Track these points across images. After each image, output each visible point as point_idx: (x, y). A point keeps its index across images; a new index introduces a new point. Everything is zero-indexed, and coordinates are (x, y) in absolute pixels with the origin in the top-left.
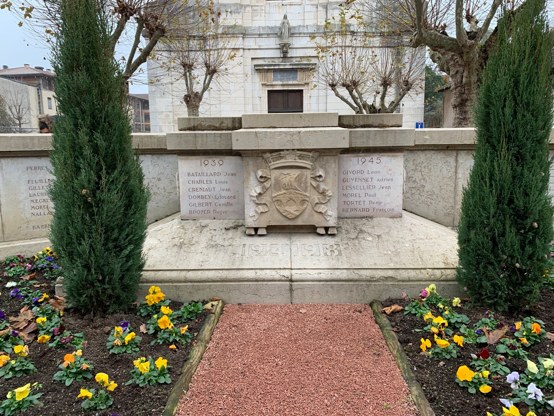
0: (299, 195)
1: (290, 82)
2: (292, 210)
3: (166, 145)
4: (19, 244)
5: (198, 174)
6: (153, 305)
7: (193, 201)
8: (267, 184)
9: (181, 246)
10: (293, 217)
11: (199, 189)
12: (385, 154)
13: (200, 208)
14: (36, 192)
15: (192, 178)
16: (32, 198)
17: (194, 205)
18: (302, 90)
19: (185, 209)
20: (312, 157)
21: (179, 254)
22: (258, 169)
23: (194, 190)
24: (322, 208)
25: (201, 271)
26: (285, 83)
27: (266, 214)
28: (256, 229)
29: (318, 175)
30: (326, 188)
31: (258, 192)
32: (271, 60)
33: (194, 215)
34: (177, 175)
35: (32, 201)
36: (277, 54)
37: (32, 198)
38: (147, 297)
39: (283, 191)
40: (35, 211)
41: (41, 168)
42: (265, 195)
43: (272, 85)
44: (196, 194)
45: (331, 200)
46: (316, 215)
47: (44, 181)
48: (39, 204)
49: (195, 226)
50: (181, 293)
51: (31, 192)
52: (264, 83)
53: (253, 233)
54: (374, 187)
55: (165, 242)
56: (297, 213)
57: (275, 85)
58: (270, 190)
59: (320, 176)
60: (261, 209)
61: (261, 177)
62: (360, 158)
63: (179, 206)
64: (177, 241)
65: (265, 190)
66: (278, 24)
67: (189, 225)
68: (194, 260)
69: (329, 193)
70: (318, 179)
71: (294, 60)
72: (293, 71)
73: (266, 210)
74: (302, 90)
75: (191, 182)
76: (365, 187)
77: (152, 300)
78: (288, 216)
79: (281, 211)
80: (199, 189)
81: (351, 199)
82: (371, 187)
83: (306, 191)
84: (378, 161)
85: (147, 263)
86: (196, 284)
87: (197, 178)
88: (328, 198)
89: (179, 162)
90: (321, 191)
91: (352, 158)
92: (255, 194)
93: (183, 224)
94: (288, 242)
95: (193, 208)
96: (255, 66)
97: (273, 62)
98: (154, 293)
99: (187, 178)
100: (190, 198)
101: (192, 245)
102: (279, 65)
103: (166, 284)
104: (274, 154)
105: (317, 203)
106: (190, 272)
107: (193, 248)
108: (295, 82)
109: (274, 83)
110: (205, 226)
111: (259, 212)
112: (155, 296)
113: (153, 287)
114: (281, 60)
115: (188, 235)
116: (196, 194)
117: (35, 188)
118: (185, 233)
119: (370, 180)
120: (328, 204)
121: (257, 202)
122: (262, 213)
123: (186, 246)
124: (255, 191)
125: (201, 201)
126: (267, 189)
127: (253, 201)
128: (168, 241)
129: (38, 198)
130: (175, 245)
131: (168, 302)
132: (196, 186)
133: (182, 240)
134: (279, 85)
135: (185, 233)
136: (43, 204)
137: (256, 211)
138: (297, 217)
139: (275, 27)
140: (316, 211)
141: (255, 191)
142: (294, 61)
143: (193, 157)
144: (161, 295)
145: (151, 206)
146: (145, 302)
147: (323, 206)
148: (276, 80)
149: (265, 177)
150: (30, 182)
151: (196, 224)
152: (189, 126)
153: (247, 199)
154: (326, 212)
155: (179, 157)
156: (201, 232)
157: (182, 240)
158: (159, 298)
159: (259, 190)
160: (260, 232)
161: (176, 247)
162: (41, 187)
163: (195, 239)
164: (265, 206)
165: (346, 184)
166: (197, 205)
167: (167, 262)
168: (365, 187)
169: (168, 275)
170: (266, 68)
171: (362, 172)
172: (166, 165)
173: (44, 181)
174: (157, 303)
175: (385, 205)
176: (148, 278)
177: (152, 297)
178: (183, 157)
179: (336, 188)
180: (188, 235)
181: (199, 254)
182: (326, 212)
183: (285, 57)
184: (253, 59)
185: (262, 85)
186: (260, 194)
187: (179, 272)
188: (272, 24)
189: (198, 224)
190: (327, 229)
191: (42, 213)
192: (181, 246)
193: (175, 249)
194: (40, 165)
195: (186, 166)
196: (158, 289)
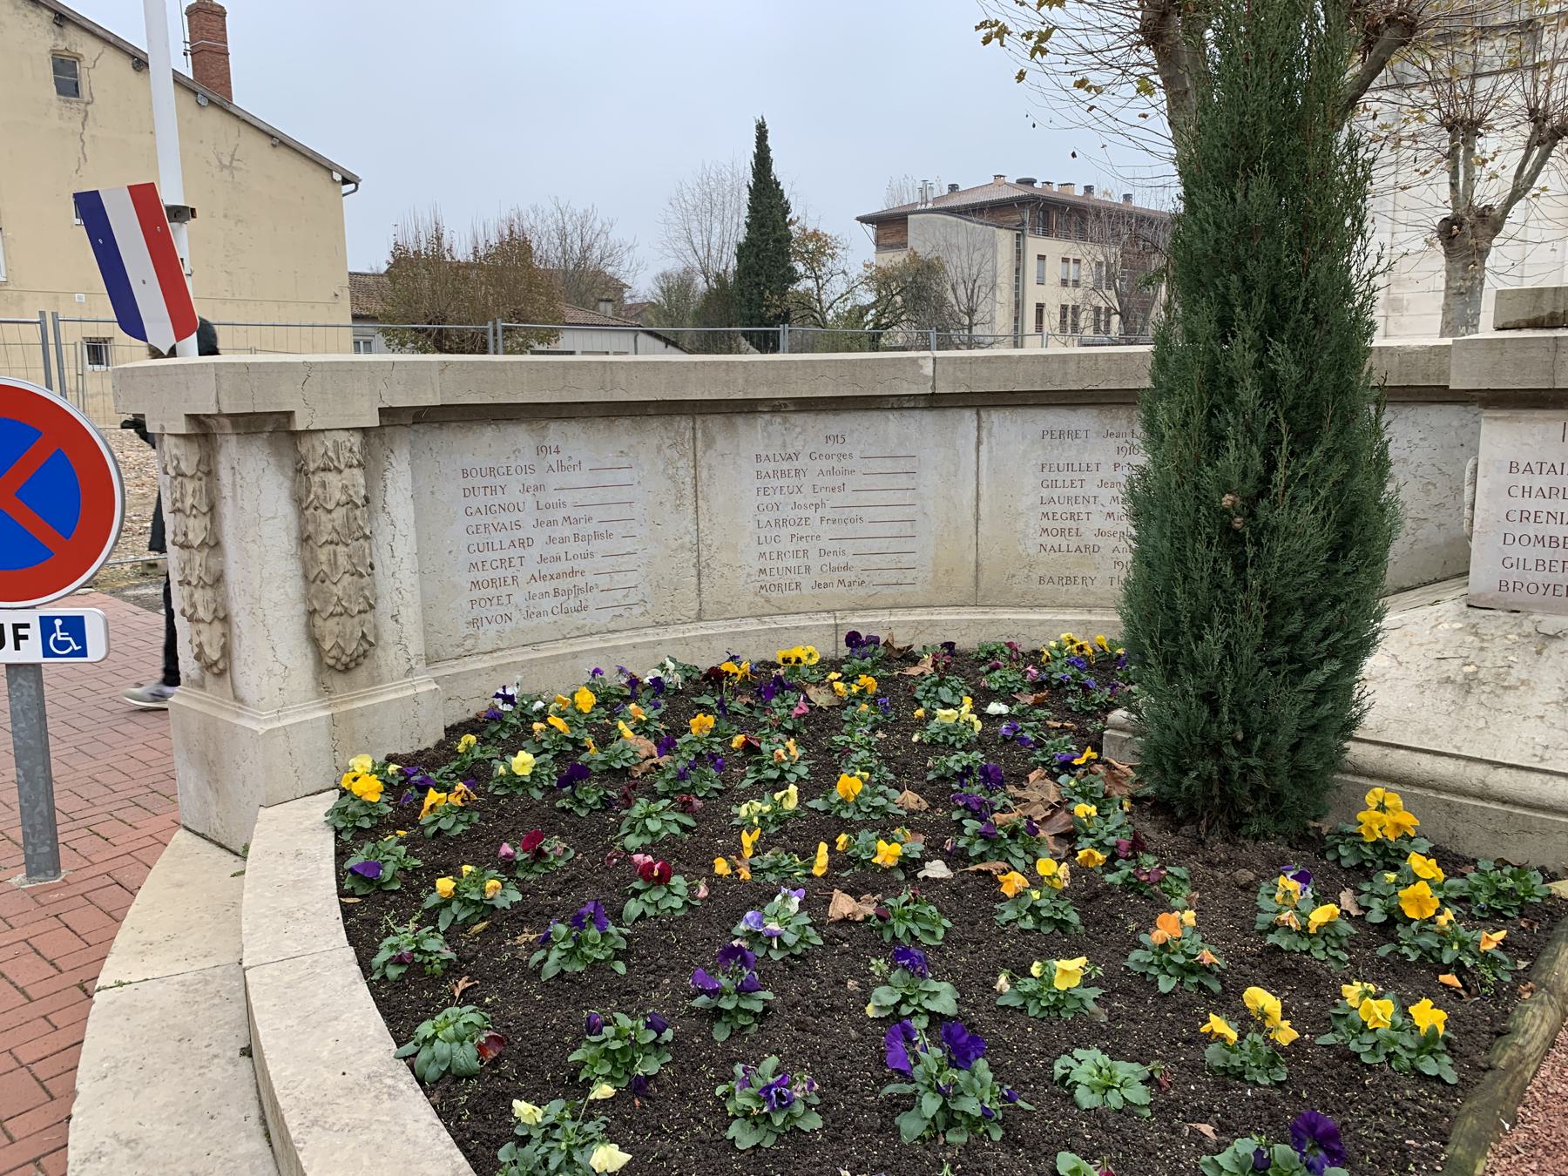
3: (1445, 373)
4: (1006, 616)
5: (1546, 468)
6: (1377, 844)
7: (1516, 552)
9: (1467, 685)
11: (1543, 517)
13: (1541, 577)
15: (1524, 480)
16: (1045, 508)
17: (1521, 564)
19: (1484, 572)
21: (1462, 708)
23: (1524, 516)
25: (1541, 776)
33: (1520, 597)
34: (1470, 464)
35: (1045, 515)
37: (1045, 508)
38: (1361, 816)
40: (1049, 541)
41: (1075, 435)
44: (1531, 529)
47: (1076, 467)
48: (1059, 525)
49: (1516, 630)
50: (1462, 829)
51: (1045, 493)
55: (1413, 667)
63: (1468, 563)
64: (1452, 668)
67: (1496, 625)
68: (1514, 736)
75: (1517, 492)
77: (1376, 827)
80: (1543, 517)
85: (1370, 720)
86: (1518, 811)
87: (1542, 481)
89: (1485, 428)
93: (1473, 621)
95: (1514, 575)
98: (1382, 808)
99: (1505, 478)
100: (1509, 540)
101: (1505, 688)
103: (1417, 791)
106: (1502, 771)
107: (1510, 699)
110: (1555, 637)
112: (1387, 819)
113: (1378, 790)
115: (1494, 657)
116: (1531, 529)
117: (1054, 484)
118: (1482, 649)
123: (1487, 689)
125: (1546, 554)
128: (1424, 665)
129: (1058, 509)
130: (1448, 680)
131: (1425, 845)
132: (1532, 504)
133: (1472, 669)
135: (1482, 649)
136: (1069, 524)
143: (1538, 414)
144: (1409, 820)
145: (1397, 551)
146: (1355, 829)
150: (1046, 469)
151: (1521, 625)
152: (1532, 316)
155: (1488, 413)
156: (1539, 653)
157: (1472, 669)
158: (1398, 826)
161: (1450, 687)
163: (1518, 673)
166: (1531, 564)
167: (1422, 727)
169: (1426, 765)
172: (1416, 436)
173: (1076, 467)
174: (1392, 838)
176: (1359, 762)
177: (1378, 820)
178: (1499, 414)
180: (1494, 657)
181: (1532, 722)
187: (1463, 763)
189: (1528, 627)
191: (1064, 548)
192: (1467, 685)
193: (1449, 693)
195: (1502, 441)
196: (1394, 800)
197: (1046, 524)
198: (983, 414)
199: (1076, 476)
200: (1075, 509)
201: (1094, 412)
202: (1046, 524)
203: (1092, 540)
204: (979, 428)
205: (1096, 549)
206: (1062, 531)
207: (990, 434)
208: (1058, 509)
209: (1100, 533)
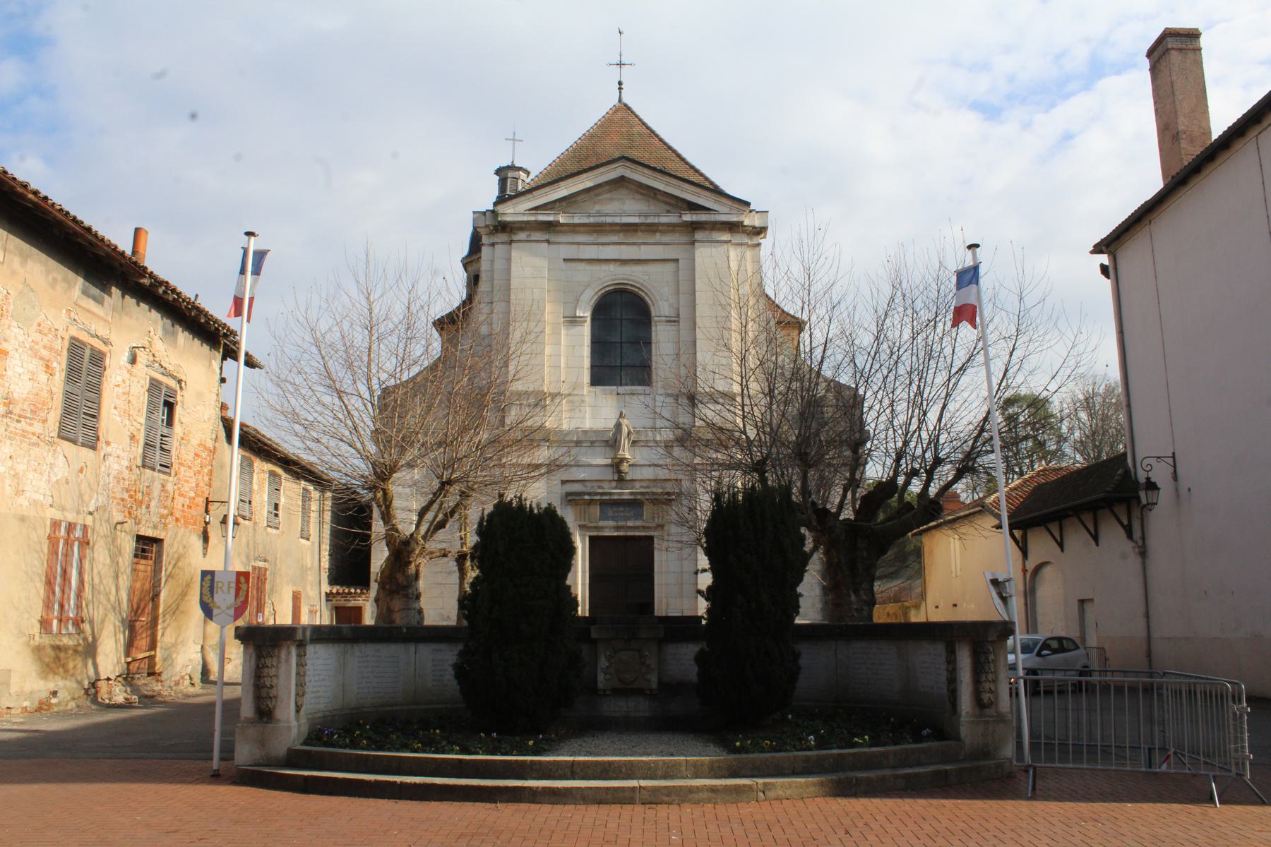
1: (630, 524)
18: (651, 538)
24: (649, 677)
26: (620, 523)
32: (595, 484)
36: (609, 475)
52: (582, 523)
57: (602, 528)
66: (611, 424)
71: (637, 485)
72: (634, 505)
74: (651, 538)
96: (568, 494)
97: (600, 487)
102: (610, 494)
108: (639, 523)
109: (601, 523)
114: (614, 484)
134: (610, 528)
139: (606, 431)
142: (638, 489)
148: (607, 519)
170: (587, 497)
183: (621, 480)
184: (563, 482)
188: (600, 425)
190: (651, 690)
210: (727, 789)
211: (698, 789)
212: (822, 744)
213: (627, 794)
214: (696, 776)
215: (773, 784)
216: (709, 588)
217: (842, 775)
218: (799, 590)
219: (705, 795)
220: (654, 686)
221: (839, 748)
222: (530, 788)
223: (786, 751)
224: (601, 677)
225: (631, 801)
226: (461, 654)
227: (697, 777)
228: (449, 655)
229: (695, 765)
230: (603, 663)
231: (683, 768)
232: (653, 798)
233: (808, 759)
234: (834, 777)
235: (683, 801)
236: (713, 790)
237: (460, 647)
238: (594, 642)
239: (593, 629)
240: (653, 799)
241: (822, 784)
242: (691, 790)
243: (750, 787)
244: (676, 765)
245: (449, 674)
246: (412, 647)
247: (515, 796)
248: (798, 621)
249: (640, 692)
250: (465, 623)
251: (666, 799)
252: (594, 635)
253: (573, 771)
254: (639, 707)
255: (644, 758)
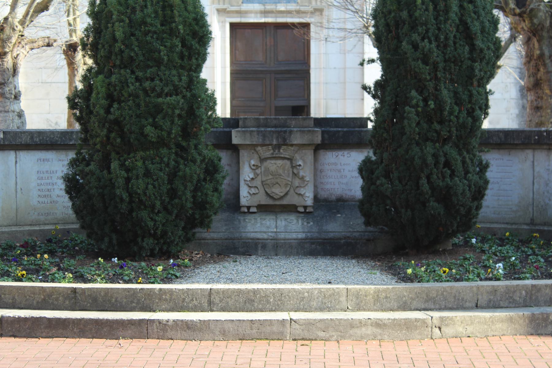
0: (284, 180)
1: (281, 7)
2: (278, 191)
8: (258, 171)
10: (278, 197)
12: (355, 150)
14: (43, 182)
16: (39, 188)
18: (306, 26)
20: (294, 150)
22: (251, 159)
24: (302, 191)
26: (269, 7)
27: (257, 195)
28: (249, 208)
29: (298, 164)
30: (304, 175)
31: (251, 177)
35: (39, 190)
37: (39, 188)
39: (271, 177)
40: (41, 200)
41: (48, 160)
42: (255, 180)
43: (239, 13)
45: (309, 185)
46: (296, 196)
48: (44, 193)
51: (39, 181)
52: (221, 6)
53: (246, 210)
54: (346, 177)
56: (282, 194)
57: (246, 12)
58: (260, 176)
59: (300, 165)
60: (253, 191)
61: (254, 165)
62: (334, 153)
65: (256, 175)
69: (307, 179)
70: (298, 167)
73: (257, 192)
74: (306, 26)
76: (339, 177)
78: (275, 197)
79: (269, 192)
81: (328, 186)
82: (343, 177)
83: (288, 176)
84: (349, 155)
88: (306, 183)
90: (301, 177)
91: (328, 153)
92: (249, 179)
94: (274, 217)
104: (264, 148)
105: (297, 187)
108: (292, 7)
109: (245, 7)
111: (252, 193)
119: (342, 170)
120: (306, 187)
121: (250, 185)
122: (254, 194)
124: (249, 177)
126: (258, 175)
127: (248, 185)
129: (43, 187)
134: (256, 13)
136: (47, 193)
137: (249, 192)
138: (282, 198)
140: (296, 193)
141: (249, 177)
147: (302, 189)
149: (257, 166)
153: (242, 183)
154: (305, 193)
159: (252, 176)
160: (251, 210)
162: (46, 178)
164: (256, 189)
165: (323, 174)
168: (339, 177)
171: (335, 164)
175: (355, 192)
179: (312, 175)
182: (305, 193)
185: (218, 11)
186: (252, 179)
190: (305, 207)
191: (46, 202)
194: (48, 158)
197: (39, 193)
198: (17, 152)
199: (49, 175)
200: (49, 187)
201: (54, 152)
202: (39, 193)
203: (55, 198)
204: (16, 158)
205: (57, 202)
206: (45, 196)
207: (20, 160)
208: (43, 187)
209: (58, 196)
210: (396, 324)
211: (361, 323)
212: (512, 273)
213: (275, 329)
214: (359, 308)
215: (451, 319)
216: (378, 84)
217: (536, 311)
218: (489, 87)
219: (369, 330)
220: (309, 202)
221: (533, 278)
222: (160, 322)
223: (468, 280)
224: (244, 192)
225: (280, 337)
226: (73, 163)
227: (359, 310)
228: (58, 164)
229: (357, 295)
230: (246, 173)
231: (343, 299)
232: (306, 335)
233: (495, 290)
234: (527, 312)
235: (343, 337)
236: (378, 324)
237: (72, 155)
238: (235, 149)
239: (234, 132)
240: (307, 335)
241: (511, 319)
242: (351, 324)
243: (424, 321)
244: (335, 294)
245: (59, 188)
246: (11, 155)
247: (141, 330)
248: (486, 125)
249: (291, 209)
250: (77, 126)
251: (321, 334)
252: (236, 140)
253: (210, 302)
254: (292, 227)
255: (296, 286)
